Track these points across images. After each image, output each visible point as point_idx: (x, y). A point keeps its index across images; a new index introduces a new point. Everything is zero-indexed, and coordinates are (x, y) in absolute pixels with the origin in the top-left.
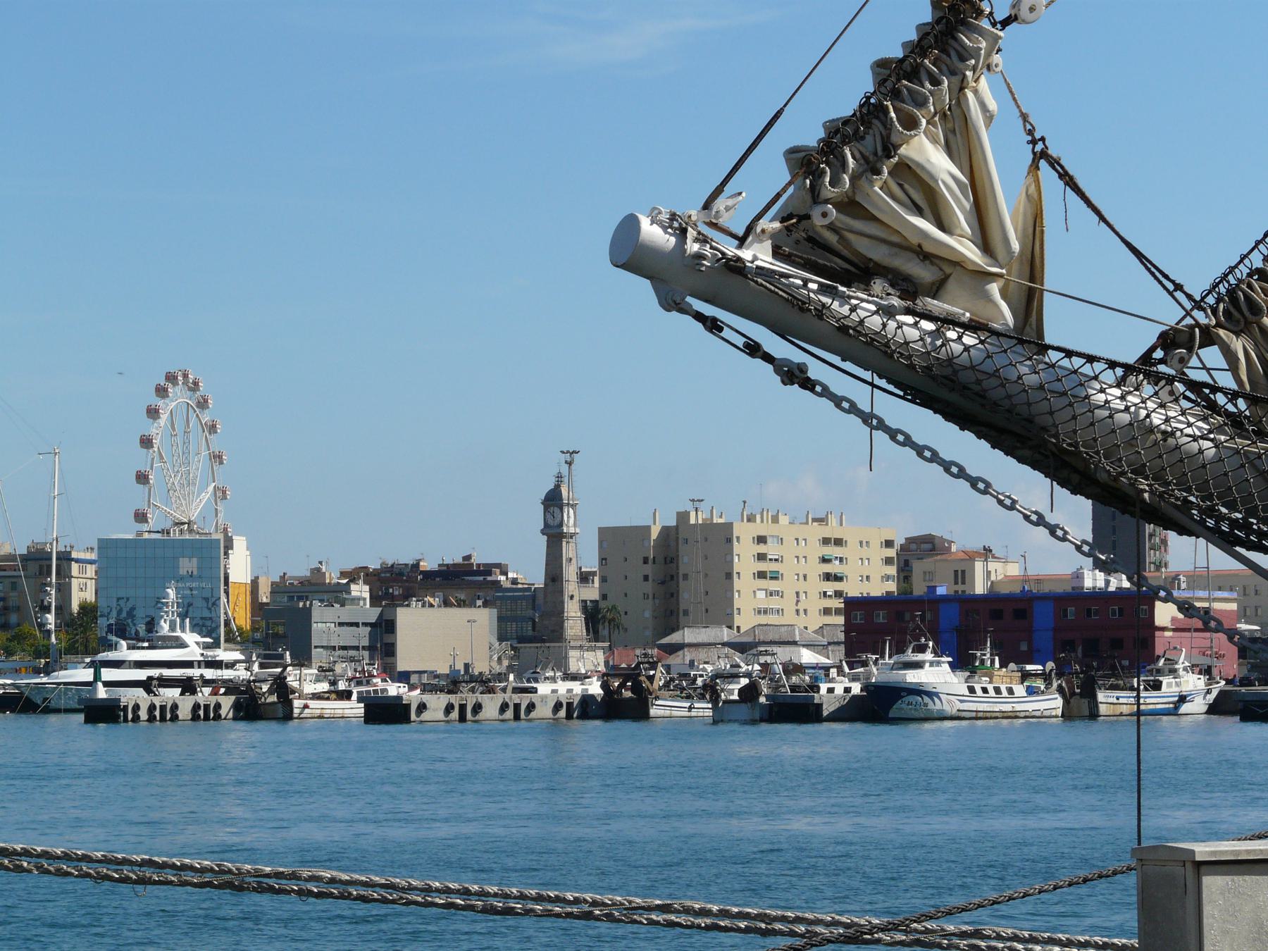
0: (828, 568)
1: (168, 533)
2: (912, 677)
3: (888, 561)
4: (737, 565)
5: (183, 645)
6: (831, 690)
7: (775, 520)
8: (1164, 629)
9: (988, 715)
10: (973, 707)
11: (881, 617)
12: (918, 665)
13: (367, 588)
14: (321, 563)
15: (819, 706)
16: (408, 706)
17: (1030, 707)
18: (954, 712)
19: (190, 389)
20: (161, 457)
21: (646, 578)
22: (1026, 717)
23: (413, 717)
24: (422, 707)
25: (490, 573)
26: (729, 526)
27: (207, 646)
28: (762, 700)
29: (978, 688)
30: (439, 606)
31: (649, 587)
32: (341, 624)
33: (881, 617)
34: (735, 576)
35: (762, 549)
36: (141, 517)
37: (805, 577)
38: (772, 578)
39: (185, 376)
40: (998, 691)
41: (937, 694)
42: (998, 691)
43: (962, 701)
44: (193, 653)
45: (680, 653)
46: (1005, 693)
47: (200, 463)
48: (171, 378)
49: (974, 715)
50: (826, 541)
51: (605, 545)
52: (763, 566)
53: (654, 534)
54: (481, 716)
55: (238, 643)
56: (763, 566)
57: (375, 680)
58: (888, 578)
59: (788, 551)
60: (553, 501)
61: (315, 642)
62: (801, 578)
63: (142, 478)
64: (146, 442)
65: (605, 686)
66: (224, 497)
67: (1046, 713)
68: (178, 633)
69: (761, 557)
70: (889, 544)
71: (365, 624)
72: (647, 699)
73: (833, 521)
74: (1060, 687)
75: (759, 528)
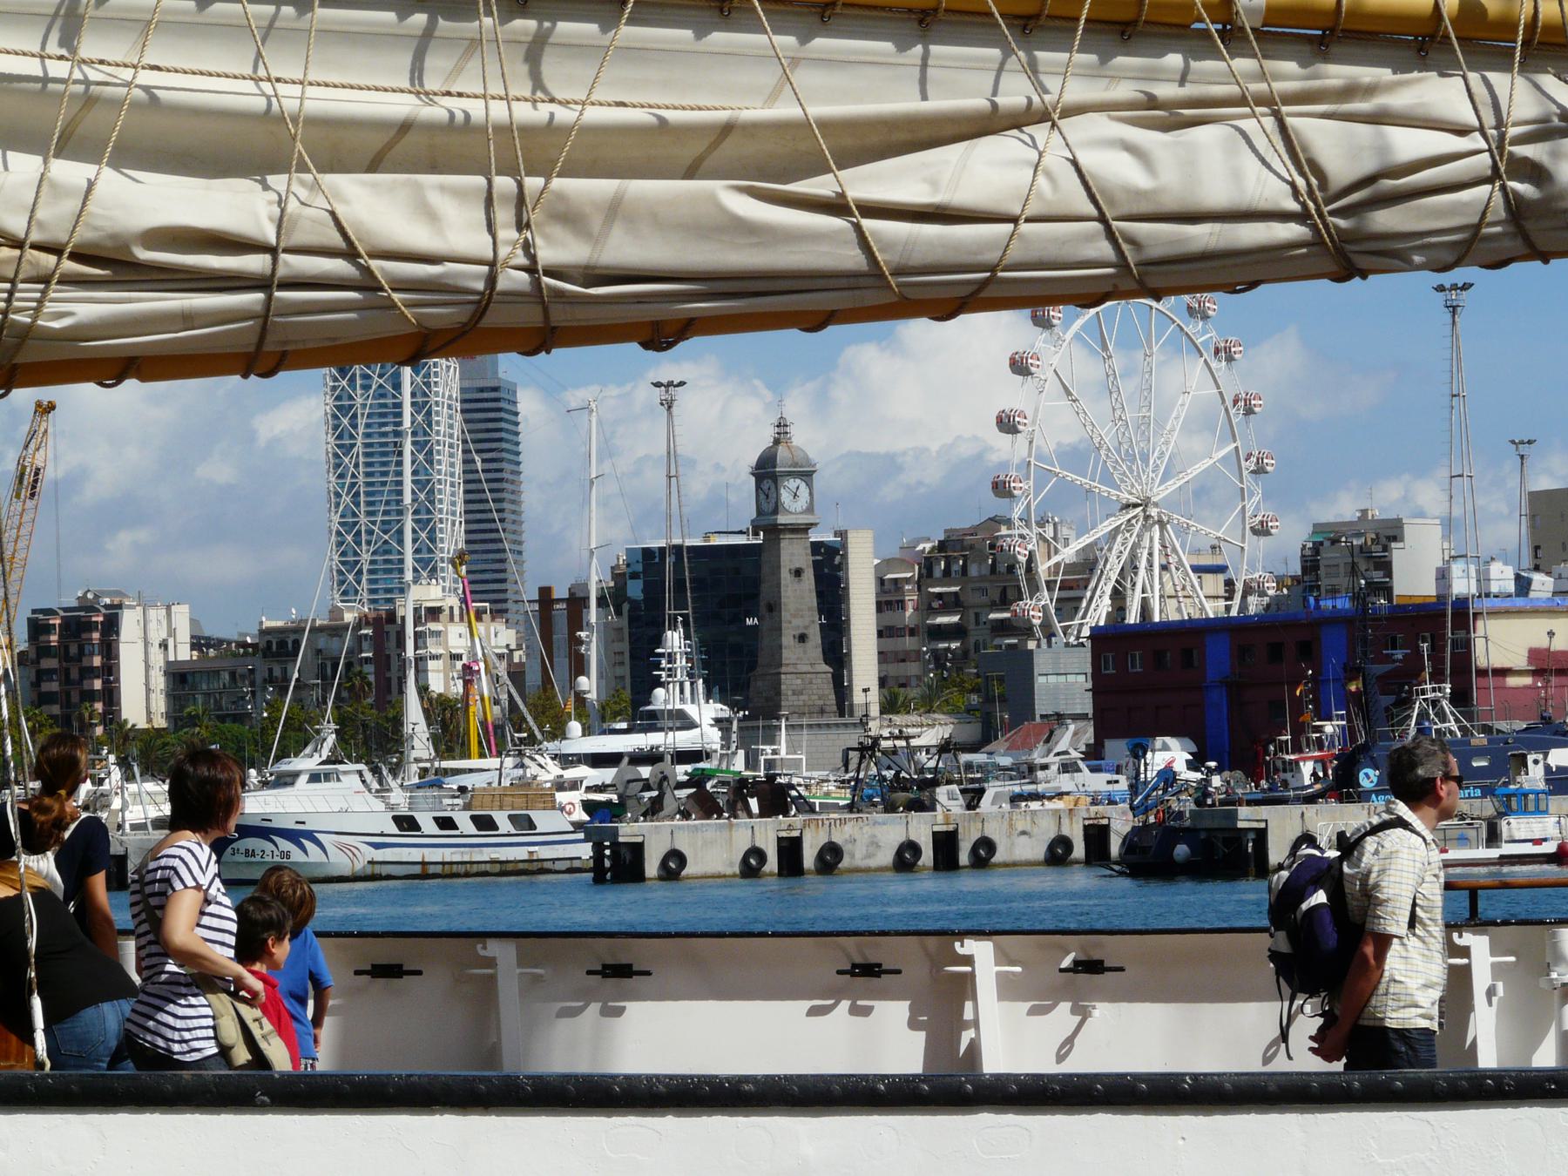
8: (1503, 672)
10: (415, 855)
18: (360, 866)
22: (570, 871)
41: (310, 836)
43: (377, 846)
46: (504, 824)
49: (417, 870)
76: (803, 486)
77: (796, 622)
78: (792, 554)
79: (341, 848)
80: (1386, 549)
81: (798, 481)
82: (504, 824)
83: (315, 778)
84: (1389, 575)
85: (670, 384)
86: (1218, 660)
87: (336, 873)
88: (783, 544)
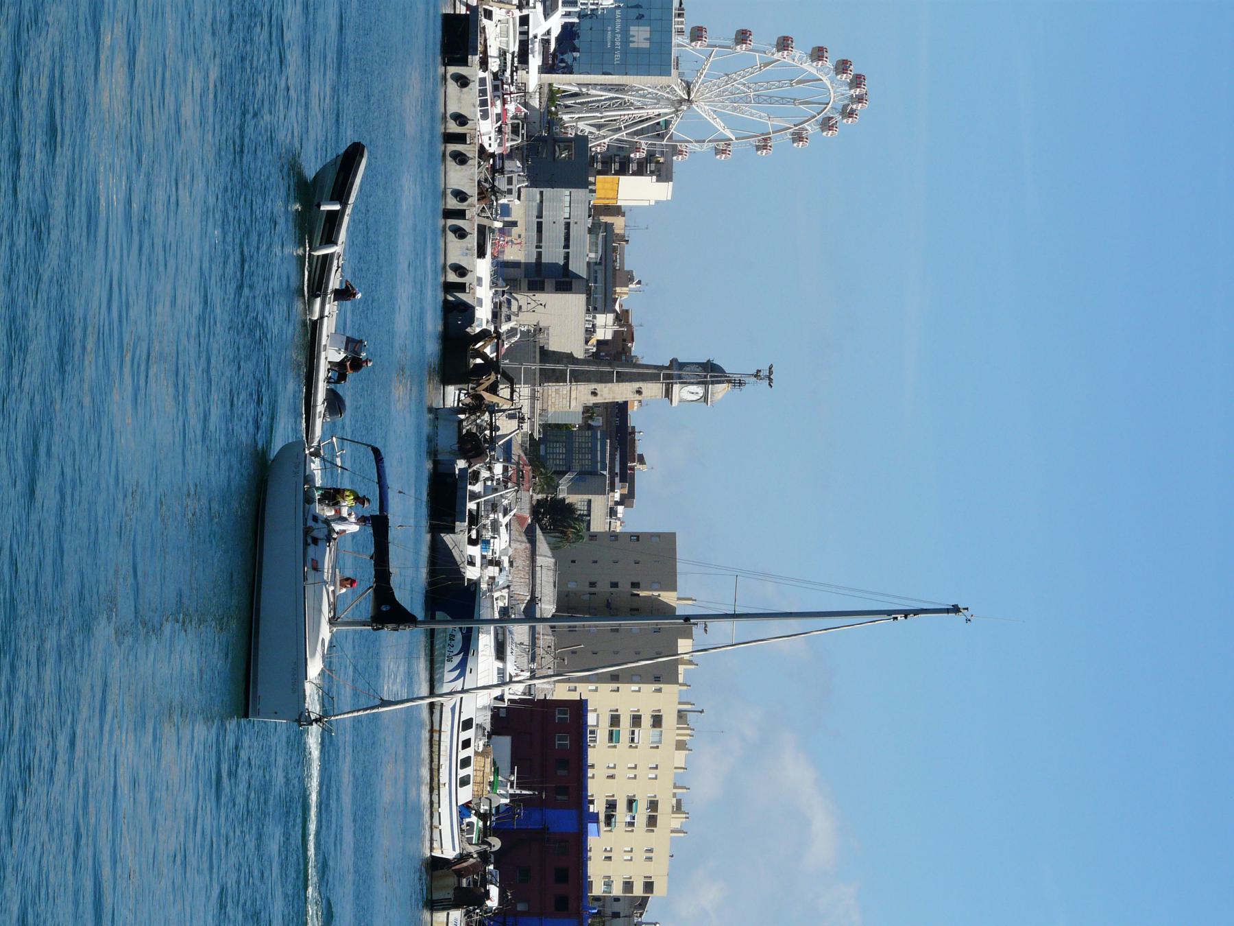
0: (622, 806)
1: (680, 15)
2: (486, 641)
3: (628, 886)
4: (627, 689)
5: (547, 15)
6: (472, 563)
7: (681, 745)
9: (435, 748)
10: (446, 727)
11: (563, 742)
12: (500, 653)
13: (609, 337)
14: (639, 283)
15: (452, 530)
16: (464, 62)
17: (444, 809)
19: (845, 106)
20: (766, 65)
21: (615, 585)
22: (432, 803)
23: (452, 70)
24: (463, 82)
25: (623, 480)
26: (674, 680)
27: (546, 42)
28: (461, 464)
29: (469, 734)
31: (603, 587)
32: (568, 225)
33: (563, 742)
34: (615, 686)
35: (646, 721)
36: (697, 34)
37: (612, 777)
38: (611, 733)
39: (860, 99)
40: (466, 763)
41: (462, 674)
42: (466, 763)
43: (453, 709)
44: (538, 25)
45: (525, 539)
46: (463, 773)
47: (760, 117)
48: (858, 81)
49: (436, 727)
50: (653, 805)
51: (656, 539)
52: (625, 722)
53: (668, 597)
54: (451, 164)
55: (548, 107)
56: (625, 722)
57: (498, 103)
58: (608, 884)
59: (643, 755)
60: (710, 372)
61: (548, 192)
62: (611, 772)
63: (743, 37)
64: (784, 44)
65: (484, 335)
66: (718, 151)
67: (436, 832)
68: (561, 10)
69: (636, 720)
70: (649, 886)
71: (567, 257)
72: (467, 382)
73: (677, 822)
74: (469, 855)
75: (670, 720)
80: (652, 173)
84: (634, 174)
85: (770, 379)
86: (560, 821)
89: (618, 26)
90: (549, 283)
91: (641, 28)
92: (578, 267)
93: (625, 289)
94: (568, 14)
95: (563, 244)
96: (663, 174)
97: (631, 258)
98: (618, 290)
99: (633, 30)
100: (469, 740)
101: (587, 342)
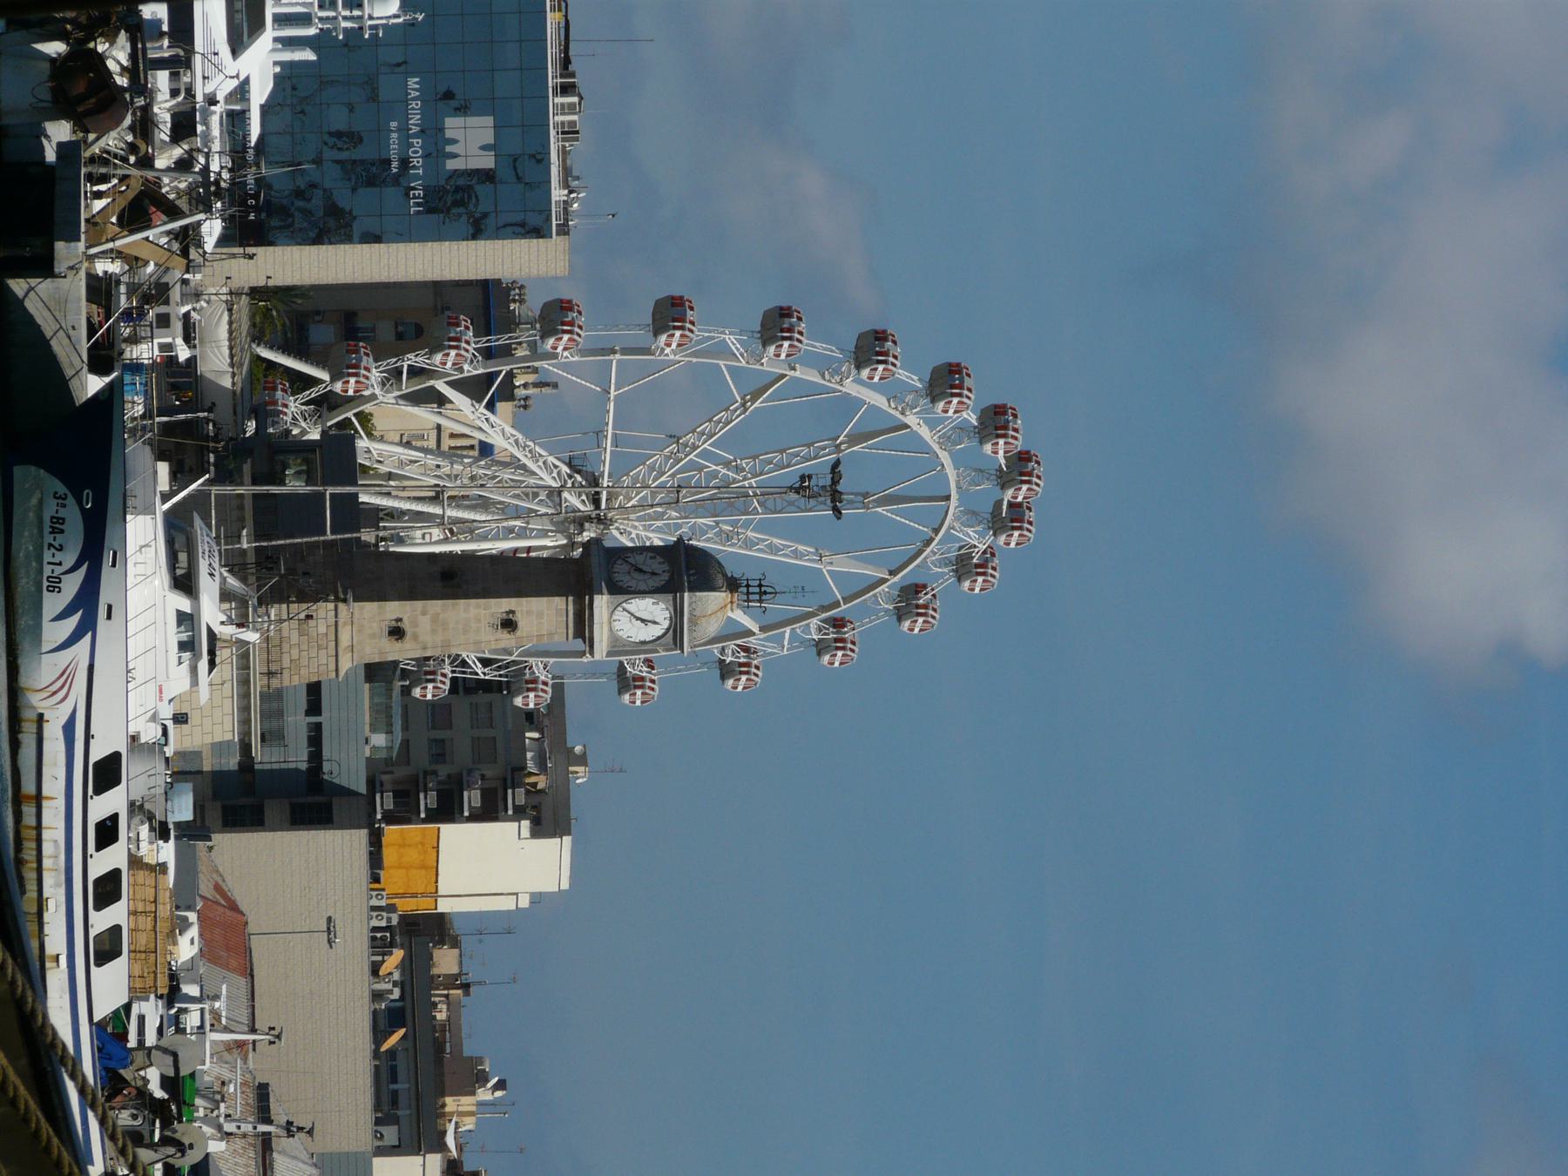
1: (566, 89)
2: (142, 536)
5: (237, 45)
10: (53, 785)
14: (501, 1085)
15: (44, 267)
18: (36, 701)
27: (236, 120)
28: (60, 131)
30: (377, 996)
40: (107, 890)
41: (87, 626)
43: (69, 728)
46: (102, 920)
49: (29, 787)
71: (315, 738)
76: (657, 631)
77: (425, 623)
78: (540, 615)
79: (66, 675)
80: (520, 813)
81: (666, 624)
82: (102, 920)
83: (186, 620)
84: (476, 817)
87: (23, 662)
88: (559, 602)
89: (415, 119)
90: (272, 810)
91: (473, 121)
92: (347, 766)
93: (467, 1103)
94: (289, 43)
95: (303, 705)
96: (547, 818)
97: (479, 1028)
98: (451, 1103)
99: (454, 125)
100: (114, 818)
101: (375, 970)
